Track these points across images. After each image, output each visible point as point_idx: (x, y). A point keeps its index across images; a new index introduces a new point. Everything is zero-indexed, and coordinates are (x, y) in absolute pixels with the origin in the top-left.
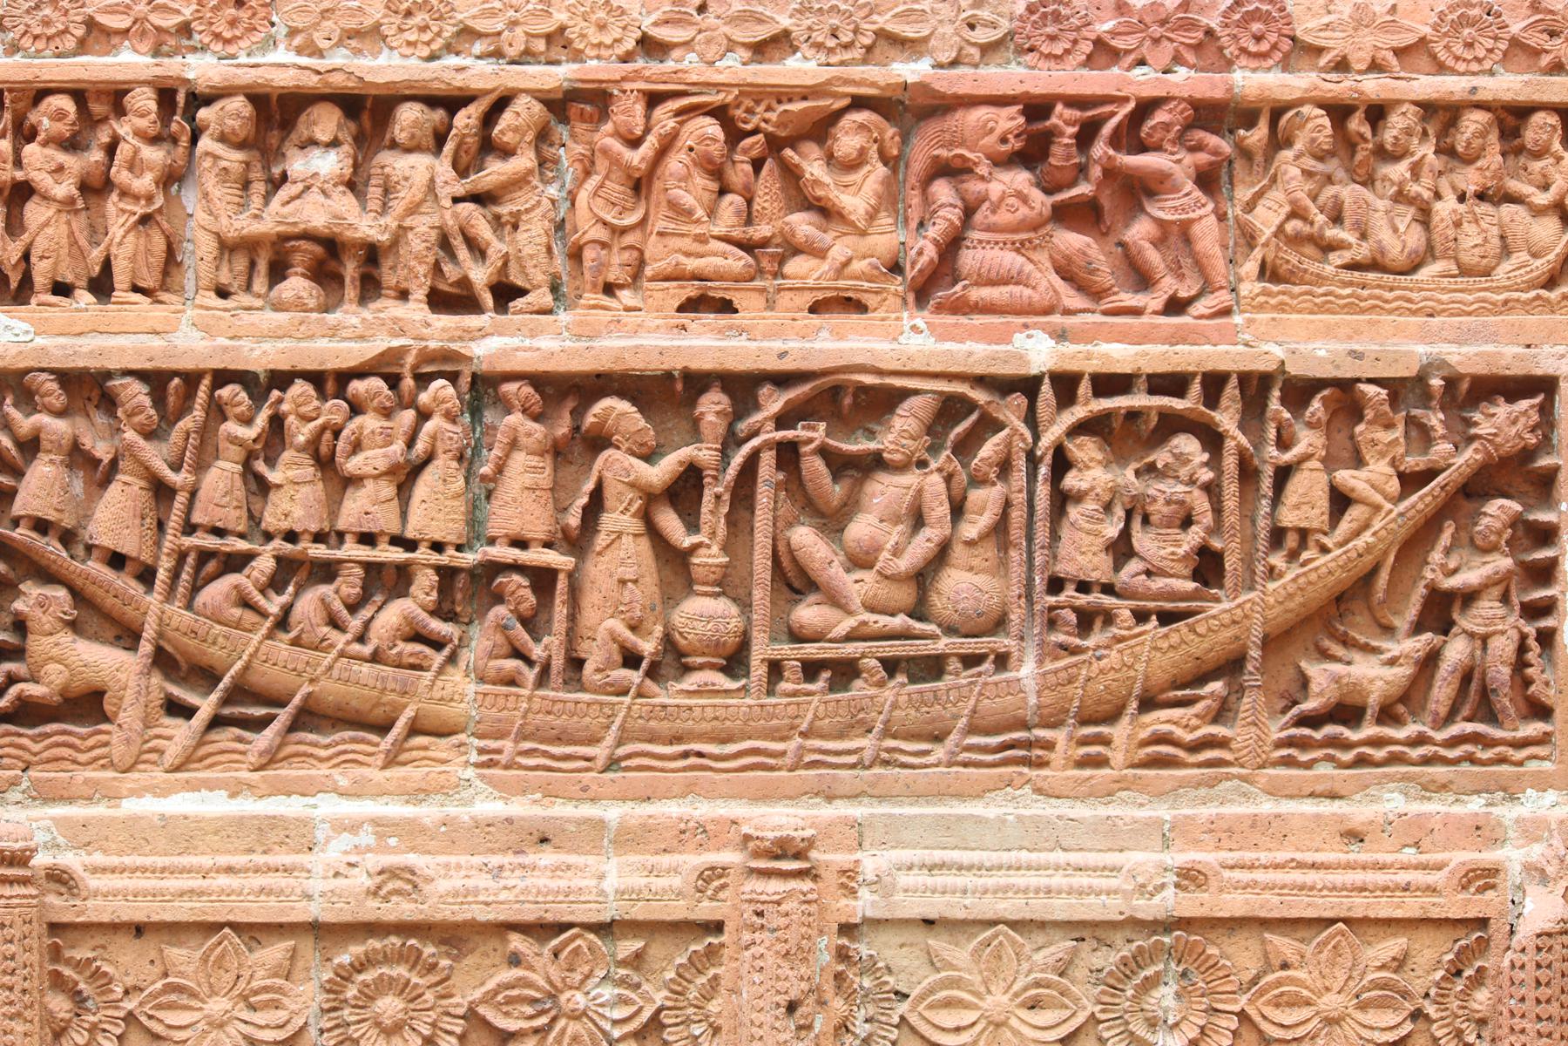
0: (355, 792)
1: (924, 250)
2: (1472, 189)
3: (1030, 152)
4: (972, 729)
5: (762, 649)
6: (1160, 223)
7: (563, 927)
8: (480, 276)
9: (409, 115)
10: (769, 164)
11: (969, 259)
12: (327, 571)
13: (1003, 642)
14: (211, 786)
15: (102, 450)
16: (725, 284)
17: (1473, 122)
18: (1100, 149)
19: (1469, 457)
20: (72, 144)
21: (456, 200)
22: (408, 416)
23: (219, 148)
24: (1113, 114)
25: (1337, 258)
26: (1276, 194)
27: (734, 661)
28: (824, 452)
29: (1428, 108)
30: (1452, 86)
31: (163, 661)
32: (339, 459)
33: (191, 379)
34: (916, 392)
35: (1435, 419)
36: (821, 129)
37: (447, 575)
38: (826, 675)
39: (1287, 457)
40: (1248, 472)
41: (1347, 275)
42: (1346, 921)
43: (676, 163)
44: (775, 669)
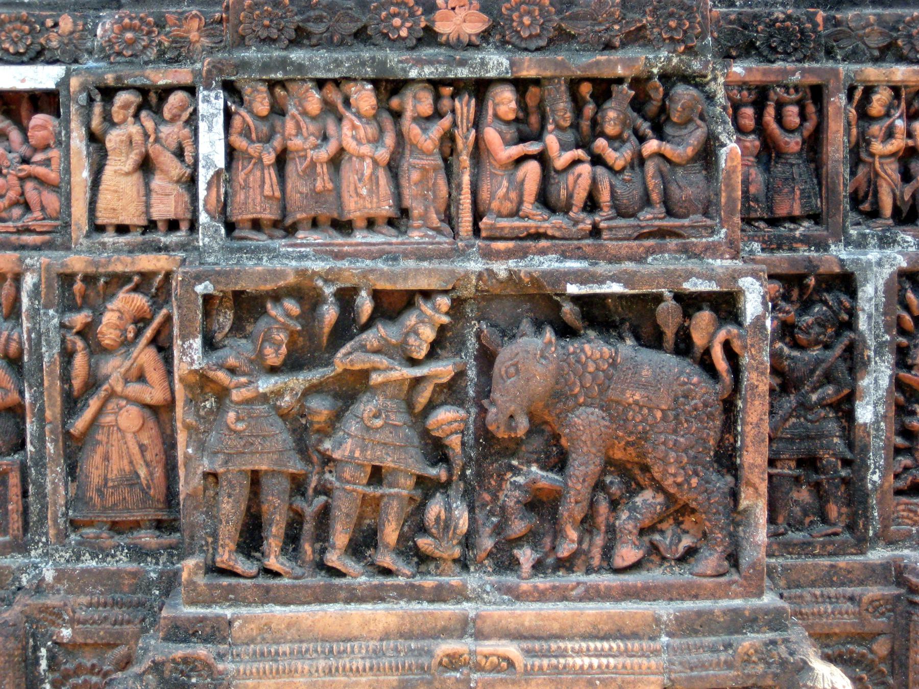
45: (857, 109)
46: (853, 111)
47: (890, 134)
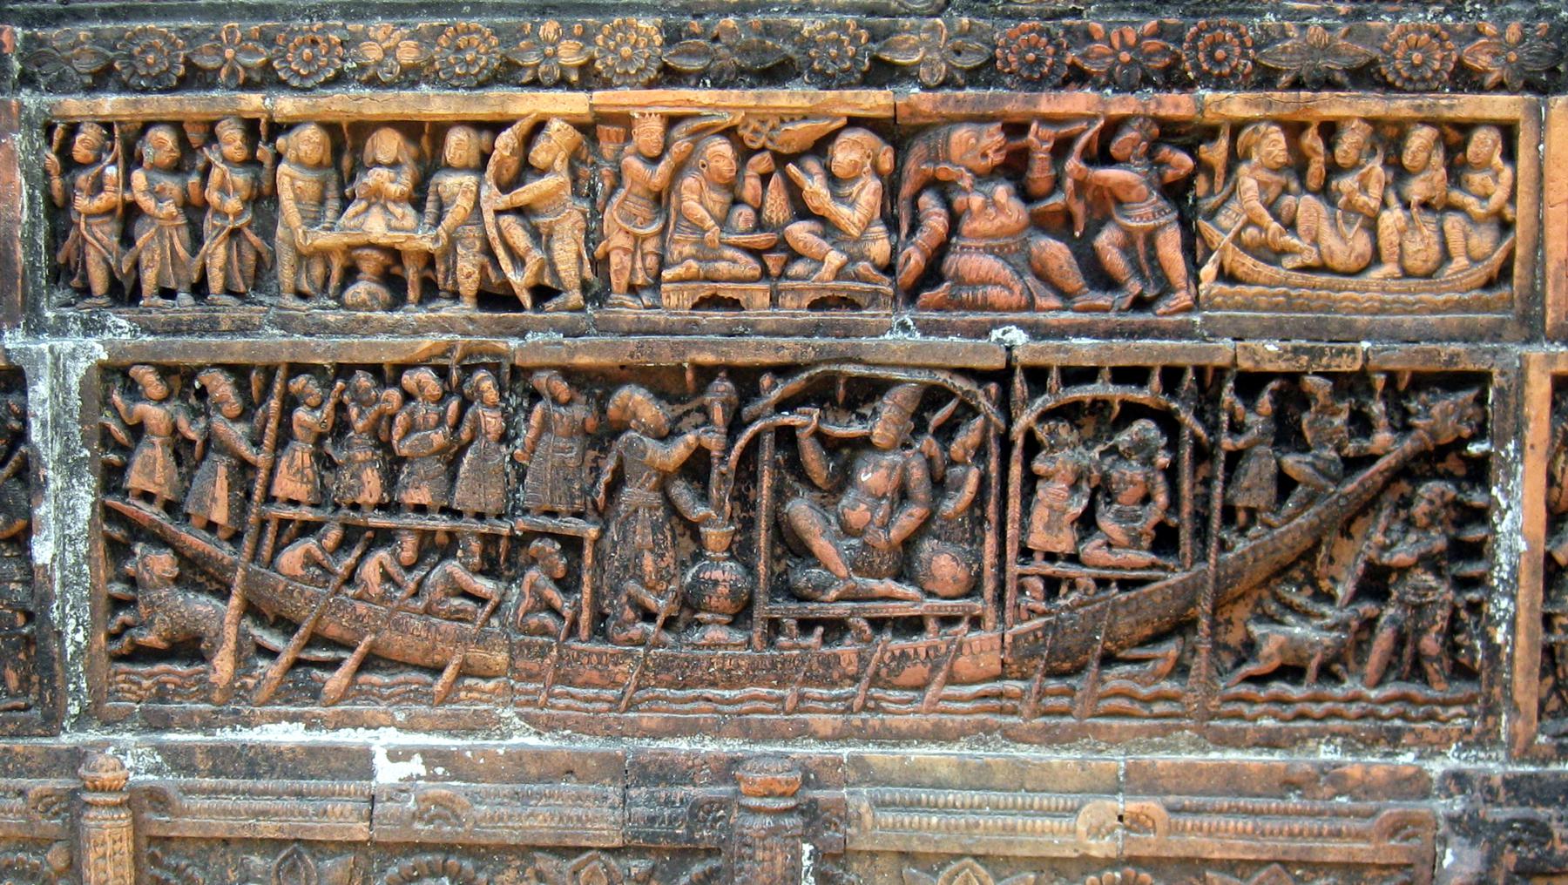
0: (410, 727)
1: (914, 259)
2: (1415, 199)
3: (1014, 168)
4: (951, 680)
5: (762, 610)
6: (1128, 233)
7: (581, 850)
8: (519, 280)
9: (458, 144)
10: (776, 179)
11: (952, 262)
12: (385, 537)
13: (977, 605)
14: (293, 718)
15: (193, 433)
16: (732, 286)
17: (1420, 138)
18: (1073, 163)
19: (1408, 445)
20: (176, 169)
21: (498, 213)
22: (454, 405)
23: (294, 171)
24: (1084, 131)
25: (1288, 262)
26: (1234, 205)
27: (741, 616)
28: (819, 435)
29: (1374, 122)
30: (1401, 106)
31: (251, 610)
32: (396, 438)
33: (269, 371)
34: (898, 383)
35: (1377, 408)
36: (821, 147)
37: (490, 540)
38: (819, 630)
39: (1241, 442)
40: (1203, 453)
41: (1297, 278)
42: (1280, 862)
43: (689, 182)
44: (775, 626)
45: (59, 153)
46: (53, 156)
47: (98, 187)
